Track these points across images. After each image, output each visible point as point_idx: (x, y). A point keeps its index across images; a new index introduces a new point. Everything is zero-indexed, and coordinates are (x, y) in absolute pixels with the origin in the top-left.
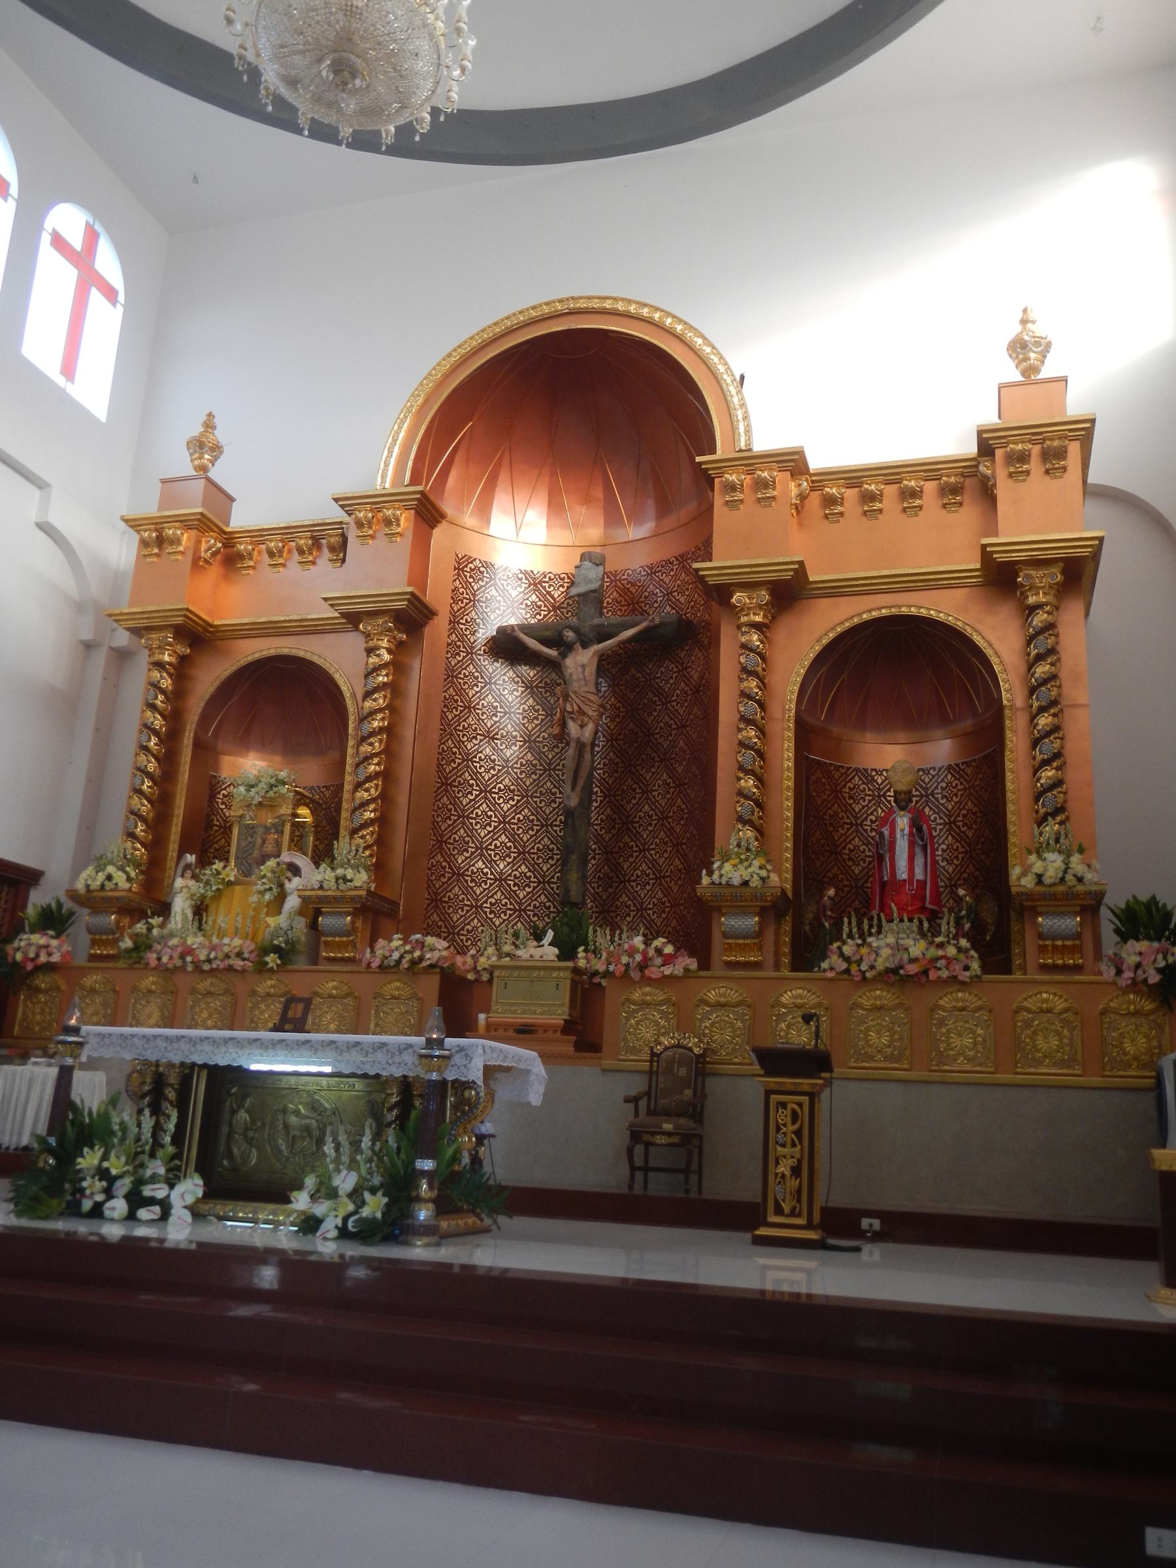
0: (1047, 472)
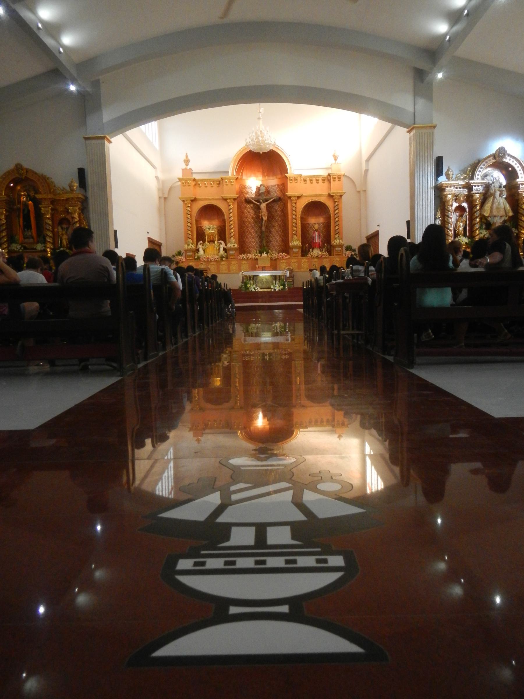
0: (338, 180)
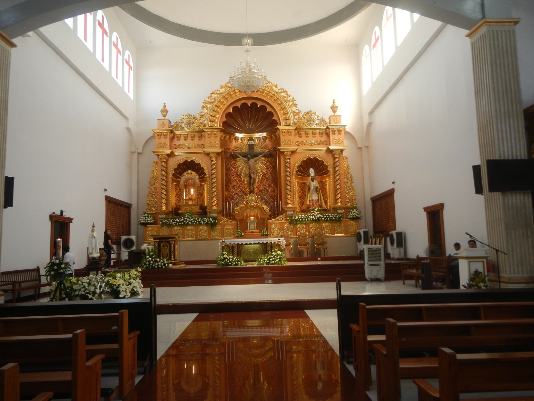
0: (338, 134)
